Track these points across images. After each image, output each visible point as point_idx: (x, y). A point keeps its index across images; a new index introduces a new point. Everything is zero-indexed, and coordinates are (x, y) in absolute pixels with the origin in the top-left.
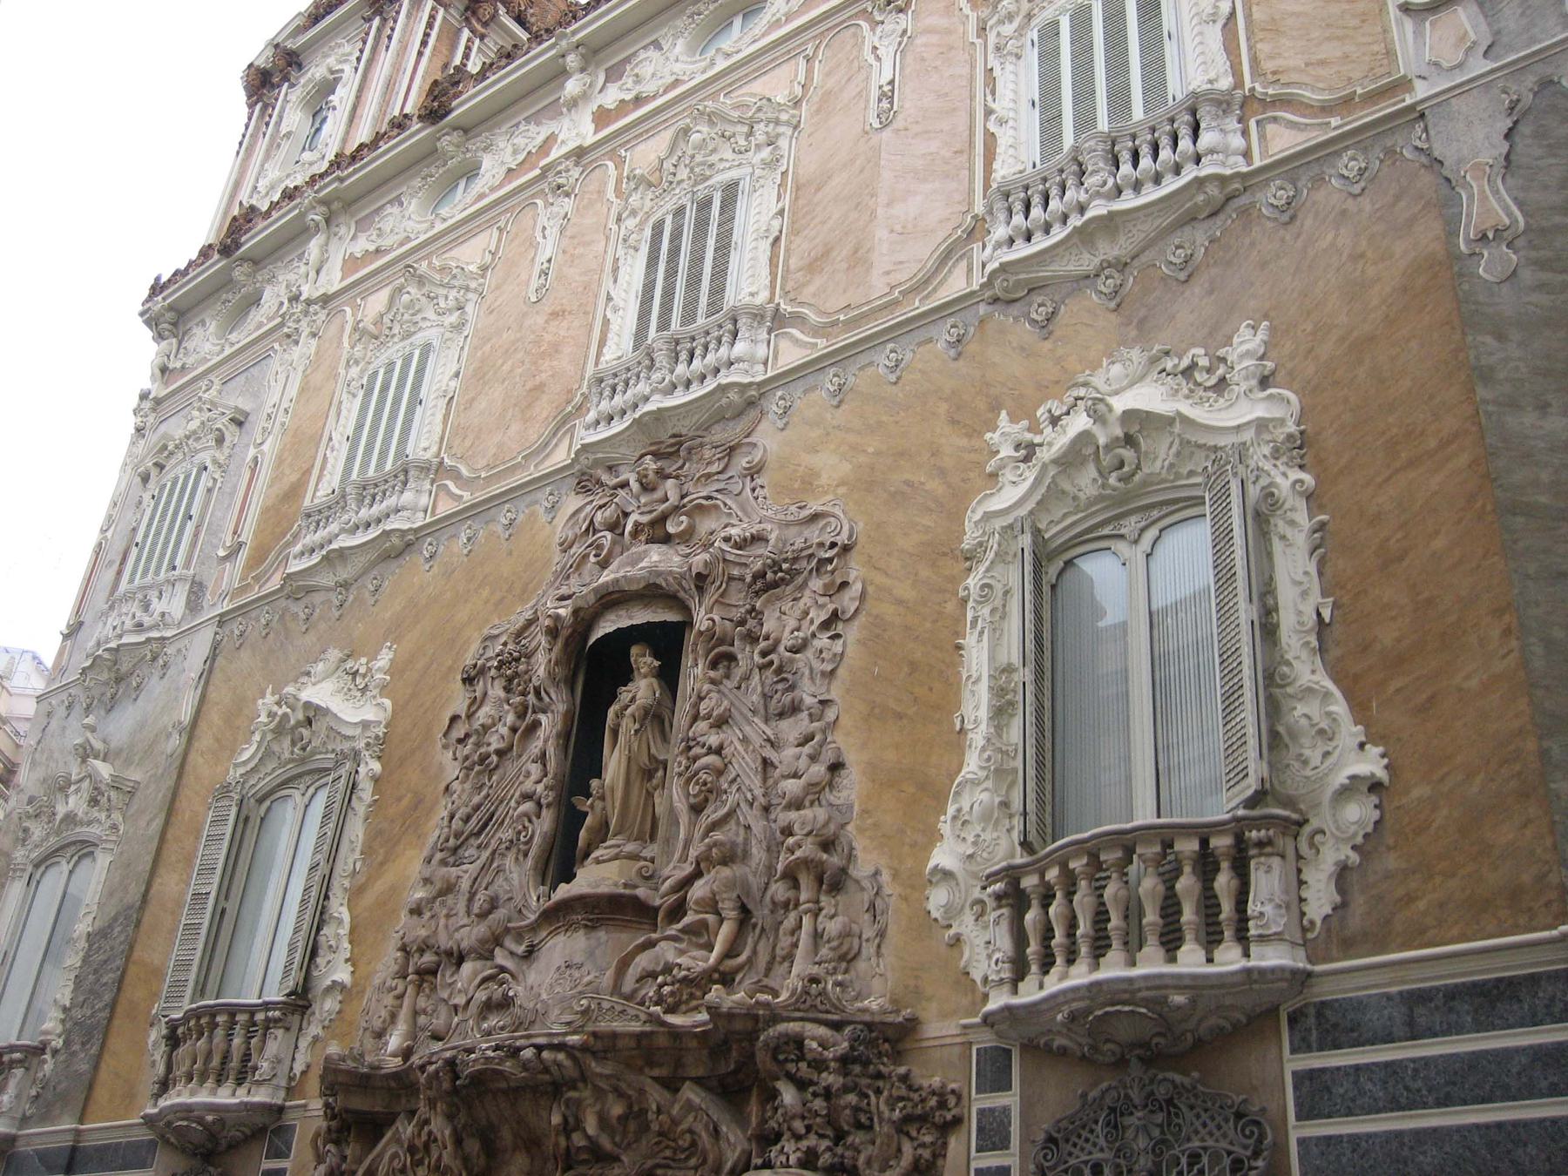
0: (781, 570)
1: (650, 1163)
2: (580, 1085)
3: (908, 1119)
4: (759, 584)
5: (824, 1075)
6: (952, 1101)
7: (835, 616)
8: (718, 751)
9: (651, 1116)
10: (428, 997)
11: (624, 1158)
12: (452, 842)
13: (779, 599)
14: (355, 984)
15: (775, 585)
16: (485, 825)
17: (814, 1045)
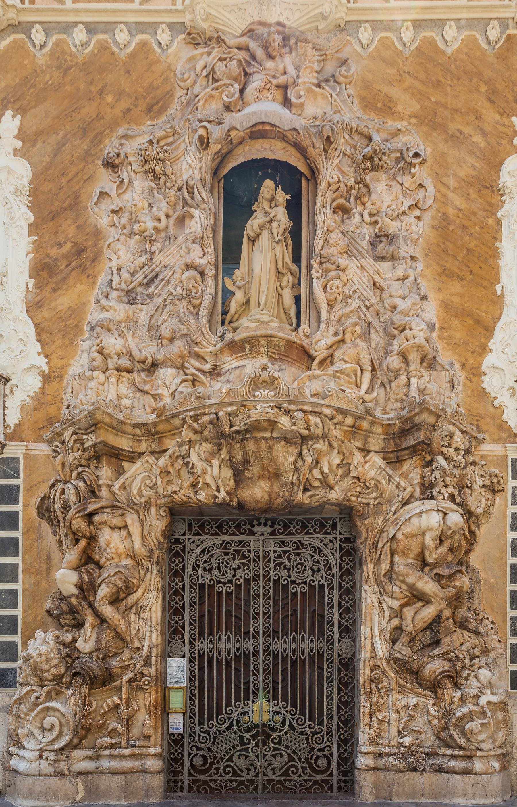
12: (124, 286)
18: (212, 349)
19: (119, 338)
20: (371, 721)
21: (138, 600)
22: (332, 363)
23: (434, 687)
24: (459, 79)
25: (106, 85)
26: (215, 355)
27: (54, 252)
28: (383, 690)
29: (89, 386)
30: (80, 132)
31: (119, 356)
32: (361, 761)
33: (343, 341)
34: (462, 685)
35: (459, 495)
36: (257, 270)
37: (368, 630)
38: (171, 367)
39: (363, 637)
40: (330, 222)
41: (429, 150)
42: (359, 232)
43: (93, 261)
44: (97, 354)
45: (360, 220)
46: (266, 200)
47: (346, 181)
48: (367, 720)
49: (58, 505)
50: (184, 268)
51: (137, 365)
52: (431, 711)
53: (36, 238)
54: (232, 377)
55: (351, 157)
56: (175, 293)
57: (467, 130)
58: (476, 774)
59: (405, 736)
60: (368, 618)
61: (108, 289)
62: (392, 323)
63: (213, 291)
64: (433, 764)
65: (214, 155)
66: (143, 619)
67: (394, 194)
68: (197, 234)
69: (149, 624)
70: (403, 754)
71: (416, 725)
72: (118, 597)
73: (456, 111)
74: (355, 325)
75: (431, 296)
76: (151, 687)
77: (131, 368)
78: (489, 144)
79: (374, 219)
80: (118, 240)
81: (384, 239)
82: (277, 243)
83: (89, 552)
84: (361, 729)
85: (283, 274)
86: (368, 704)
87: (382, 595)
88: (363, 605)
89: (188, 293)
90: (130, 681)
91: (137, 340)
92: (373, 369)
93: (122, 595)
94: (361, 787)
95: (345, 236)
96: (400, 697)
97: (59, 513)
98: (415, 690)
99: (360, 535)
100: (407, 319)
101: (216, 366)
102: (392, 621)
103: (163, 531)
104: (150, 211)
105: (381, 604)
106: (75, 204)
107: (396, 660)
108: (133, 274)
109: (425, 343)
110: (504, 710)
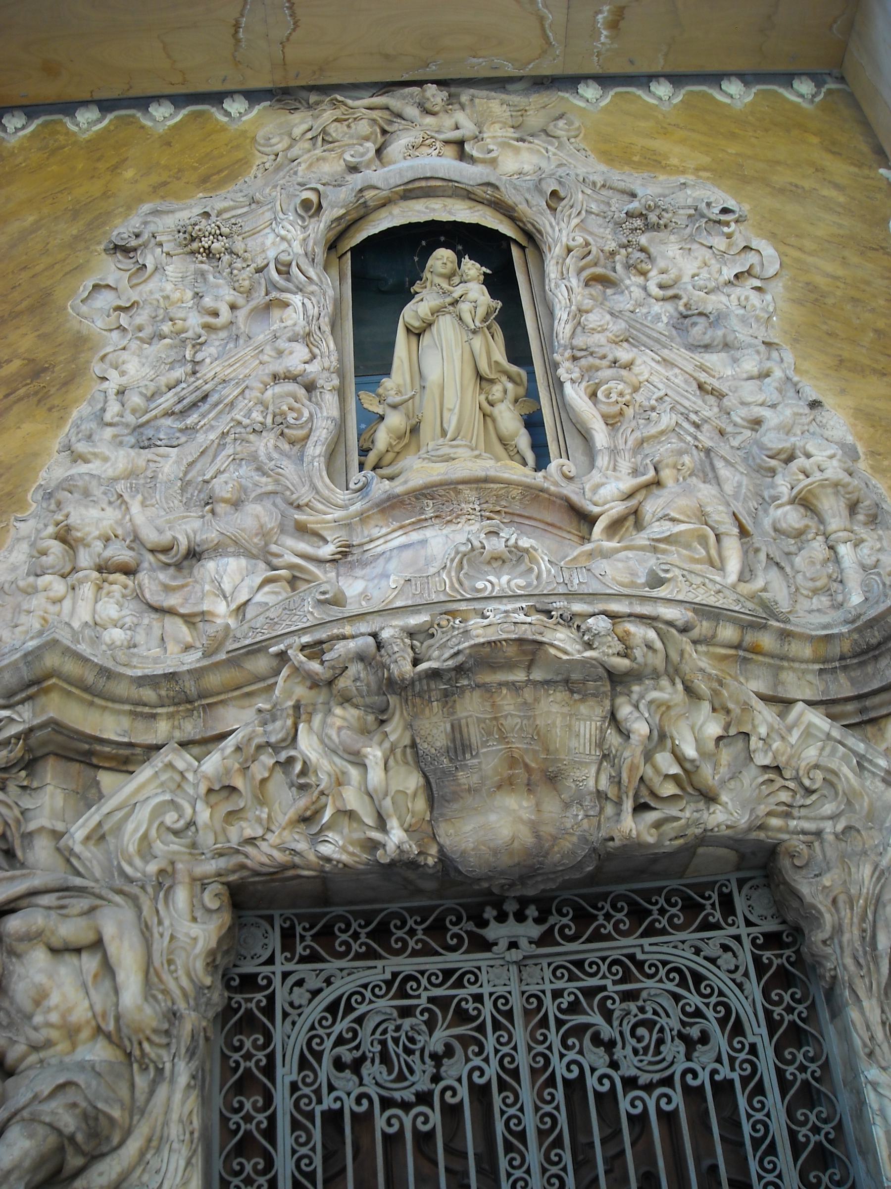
1: (762, 809)
2: (665, 682)
4: (638, 223)
7: (749, 273)
8: (628, 366)
9: (754, 742)
10: (121, 606)
11: (724, 798)
12: (130, 419)
13: (662, 242)
15: (656, 228)
18: (338, 514)
19: (109, 510)
22: (639, 525)
25: (126, 159)
26: (347, 525)
33: (657, 483)
36: (433, 370)
38: (237, 555)
42: (644, 310)
43: (66, 384)
50: (268, 380)
51: (150, 557)
55: (602, 215)
56: (246, 421)
57: (807, 184)
61: (93, 425)
62: (762, 447)
63: (335, 413)
65: (332, 222)
67: (700, 258)
68: (297, 329)
72: (59, 1170)
73: (778, 163)
74: (680, 453)
75: (828, 401)
77: (133, 563)
79: (670, 292)
80: (124, 349)
81: (702, 320)
82: (474, 332)
85: (492, 381)
89: (279, 419)
93: (74, 1161)
95: (617, 317)
99: (815, 918)
103: (212, 953)
109: (847, 479)
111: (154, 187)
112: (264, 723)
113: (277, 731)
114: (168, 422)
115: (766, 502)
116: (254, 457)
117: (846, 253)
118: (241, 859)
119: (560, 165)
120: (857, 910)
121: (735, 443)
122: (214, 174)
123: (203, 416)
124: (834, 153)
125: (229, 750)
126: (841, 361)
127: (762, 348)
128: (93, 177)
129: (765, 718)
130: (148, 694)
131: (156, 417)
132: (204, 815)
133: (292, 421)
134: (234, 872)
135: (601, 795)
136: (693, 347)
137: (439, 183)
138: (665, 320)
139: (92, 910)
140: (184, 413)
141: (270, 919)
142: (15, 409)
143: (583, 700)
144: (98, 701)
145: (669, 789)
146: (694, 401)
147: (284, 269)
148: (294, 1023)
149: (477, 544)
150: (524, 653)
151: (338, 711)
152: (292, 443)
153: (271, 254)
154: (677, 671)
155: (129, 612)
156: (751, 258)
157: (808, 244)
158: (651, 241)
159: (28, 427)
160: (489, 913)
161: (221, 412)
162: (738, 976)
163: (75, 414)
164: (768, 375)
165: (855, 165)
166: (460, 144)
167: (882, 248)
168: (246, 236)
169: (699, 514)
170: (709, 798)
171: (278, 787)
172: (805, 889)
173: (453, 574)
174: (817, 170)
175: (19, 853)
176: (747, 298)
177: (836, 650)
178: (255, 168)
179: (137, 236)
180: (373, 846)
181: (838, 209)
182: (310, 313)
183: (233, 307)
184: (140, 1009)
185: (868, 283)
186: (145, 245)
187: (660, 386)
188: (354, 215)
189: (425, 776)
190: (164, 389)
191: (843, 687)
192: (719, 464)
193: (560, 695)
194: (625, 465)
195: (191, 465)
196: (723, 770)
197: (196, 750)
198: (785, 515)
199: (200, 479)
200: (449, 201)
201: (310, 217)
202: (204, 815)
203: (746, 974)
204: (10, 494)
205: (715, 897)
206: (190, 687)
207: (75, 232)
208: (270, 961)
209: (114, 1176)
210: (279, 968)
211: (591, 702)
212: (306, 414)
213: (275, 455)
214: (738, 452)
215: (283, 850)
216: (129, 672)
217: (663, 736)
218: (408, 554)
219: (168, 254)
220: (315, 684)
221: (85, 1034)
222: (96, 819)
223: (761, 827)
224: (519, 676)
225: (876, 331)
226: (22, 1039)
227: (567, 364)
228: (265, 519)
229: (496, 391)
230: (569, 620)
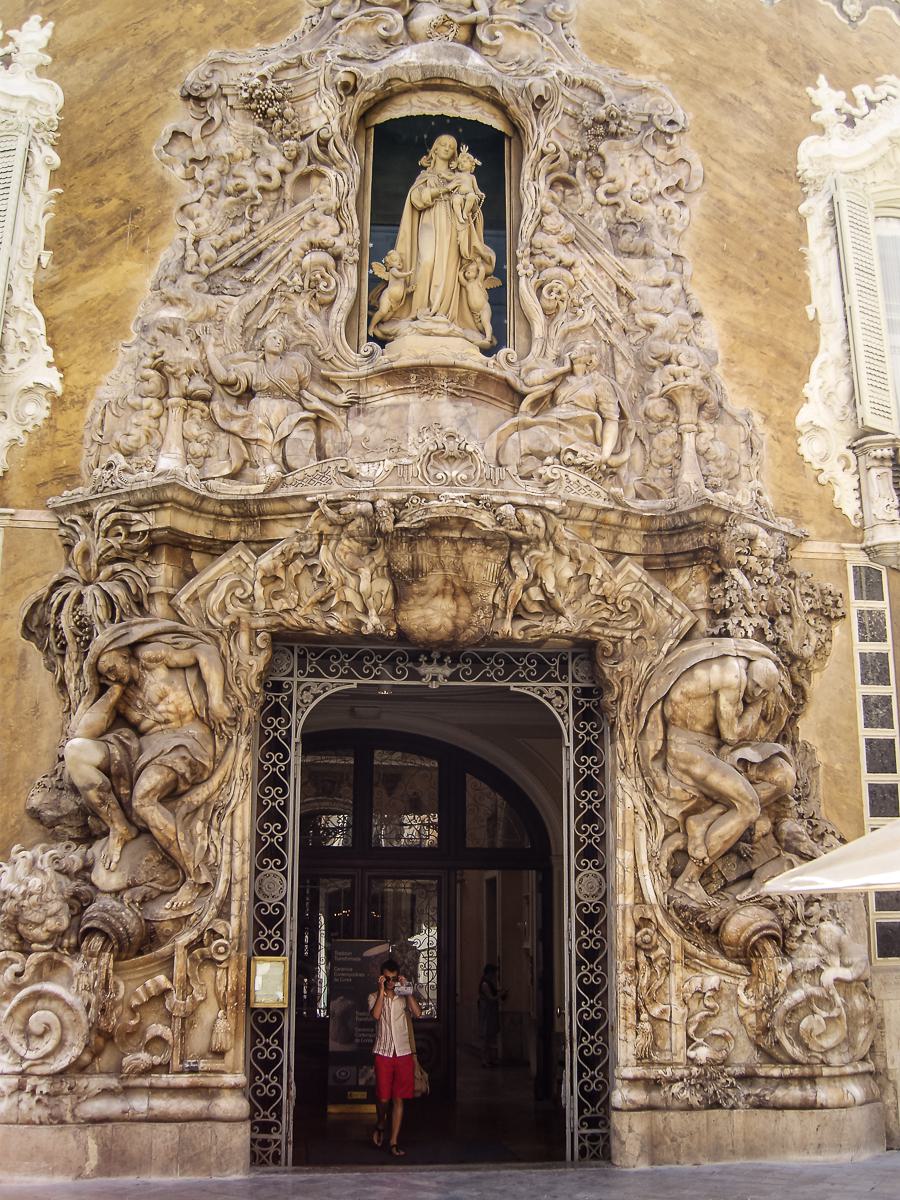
0: (620, 125)
1: (591, 622)
2: (543, 545)
3: (812, 610)
4: (601, 130)
5: (767, 569)
6: (840, 604)
8: (569, 267)
9: (593, 581)
11: (569, 613)
12: (204, 269)
13: (617, 149)
14: (68, 392)
15: (615, 136)
16: (251, 260)
17: (764, 545)
19: (191, 349)
20: (638, 1020)
21: (210, 796)
23: (747, 954)
24: (727, 32)
26: (358, 381)
27: (90, 211)
28: (659, 963)
29: (135, 421)
30: (147, 51)
31: (190, 375)
32: (620, 1096)
33: (572, 372)
34: (792, 950)
35: (772, 628)
36: (427, 255)
37: (629, 855)
38: (278, 398)
39: (620, 868)
40: (544, 201)
41: (690, 116)
44: (152, 372)
45: (592, 199)
46: (443, 159)
47: (568, 146)
48: (632, 1019)
49: (66, 622)
52: (743, 998)
53: (60, 191)
54: (385, 419)
56: (289, 283)
57: (744, 96)
58: (822, 1107)
59: (699, 1045)
60: (628, 835)
62: (650, 349)
63: (355, 285)
64: (749, 1095)
66: (219, 830)
67: (643, 167)
69: (229, 840)
70: (698, 1077)
71: (718, 1027)
73: (726, 70)
76: (229, 958)
78: (777, 117)
79: (612, 200)
81: (631, 228)
83: (122, 707)
84: (621, 1036)
86: (631, 989)
87: (651, 794)
88: (620, 811)
90: (190, 947)
91: (220, 350)
92: (622, 415)
93: (183, 787)
94: (623, 1143)
95: (569, 219)
96: (688, 974)
97: (69, 637)
98: (713, 961)
100: (673, 347)
101: (358, 398)
102: (670, 839)
103: (260, 674)
104: (254, 163)
105: (650, 809)
106: (131, 144)
107: (680, 909)
108: (219, 251)
110: (864, 993)
111: (220, 30)
112: (300, 540)
113: (309, 545)
114: (232, 273)
115: (645, 393)
116: (292, 314)
117: (757, 174)
118: (280, 620)
119: (548, 61)
120: (634, 688)
121: (633, 341)
122: (269, 23)
123: (258, 272)
124: (774, 64)
125: (277, 554)
126: (726, 277)
127: (671, 260)
128: (167, 9)
129: (601, 567)
130: (227, 510)
131: (223, 268)
132: (259, 591)
133: (323, 289)
134: (275, 626)
135: (495, 606)
136: (618, 252)
137: (451, 83)
138: (604, 224)
139: (193, 646)
140: (244, 267)
141: (292, 649)
142: (116, 245)
143: (492, 550)
144: (196, 513)
145: (535, 608)
146: (611, 302)
147: (323, 144)
148: (303, 713)
149: (441, 446)
150: (460, 523)
151: (346, 542)
152: (322, 305)
153: (316, 124)
154: (551, 538)
155: (206, 428)
156: (682, 172)
157: (731, 162)
158: (609, 148)
159: (128, 265)
160: (423, 658)
161: (271, 270)
162: (562, 711)
163: (162, 258)
164: (669, 285)
165: (787, 79)
166: (473, 27)
167: (786, 172)
168: (293, 101)
169: (593, 401)
170: (559, 613)
171: (307, 583)
172: (606, 671)
173: (424, 466)
174: (756, 83)
175: (146, 606)
176: (670, 212)
177: (656, 524)
178: (303, 21)
179: (208, 87)
180: (360, 623)
181: (763, 128)
182: (341, 190)
183: (283, 173)
184: (221, 706)
185: (765, 205)
186: (213, 96)
187: (589, 286)
188: (381, 96)
189: (394, 586)
190: (229, 243)
191: (658, 548)
192: (618, 358)
193: (479, 547)
194: (552, 353)
195: (248, 314)
196: (571, 596)
197: (254, 547)
198: (654, 407)
199: (255, 327)
200: (457, 96)
201: (346, 96)
202: (259, 591)
203: (567, 711)
204: (116, 322)
205: (557, 662)
206: (254, 509)
207: (155, 71)
208: (291, 674)
209: (205, 796)
210: (296, 679)
211: (497, 552)
212: (333, 284)
213: (310, 315)
214: (634, 348)
215: (306, 619)
216: (214, 496)
217: (536, 576)
218: (395, 413)
219: (231, 107)
220: (332, 524)
221: (189, 718)
222: (194, 588)
223: (589, 632)
224: (456, 534)
225: (759, 252)
226: (152, 717)
227: (526, 261)
228: (302, 369)
229: (472, 270)
230: (492, 507)
